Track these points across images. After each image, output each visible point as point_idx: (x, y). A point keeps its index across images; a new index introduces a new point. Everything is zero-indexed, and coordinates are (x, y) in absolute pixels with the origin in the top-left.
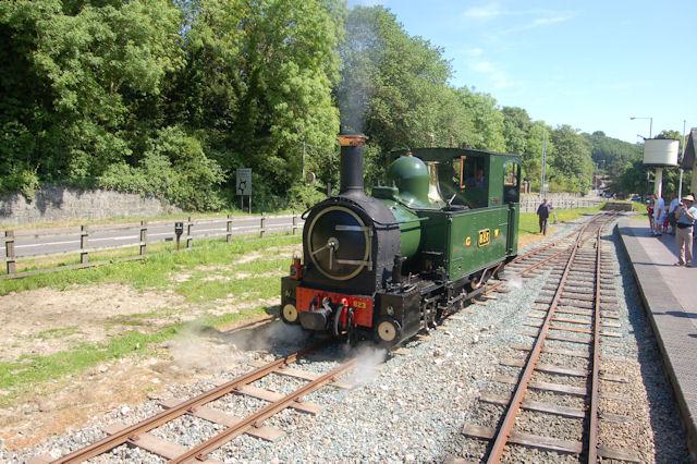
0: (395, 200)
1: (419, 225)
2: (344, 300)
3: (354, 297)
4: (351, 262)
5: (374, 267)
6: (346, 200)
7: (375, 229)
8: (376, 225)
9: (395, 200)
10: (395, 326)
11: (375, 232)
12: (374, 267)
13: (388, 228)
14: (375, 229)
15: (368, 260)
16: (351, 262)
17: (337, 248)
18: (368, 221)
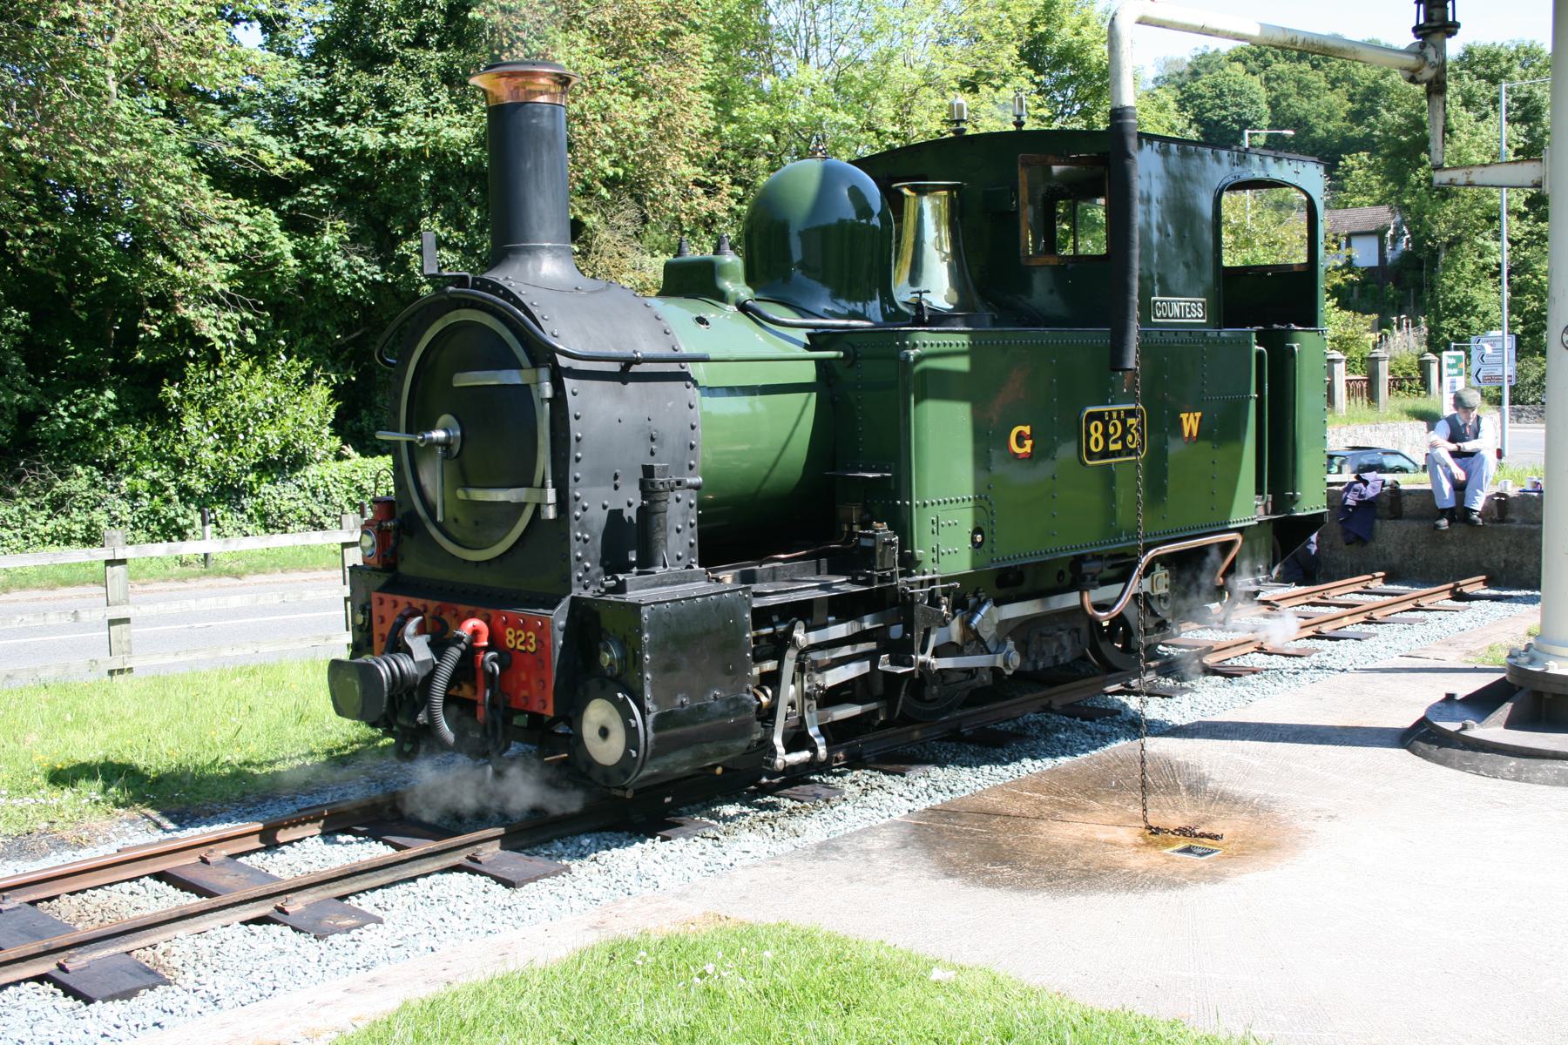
0: (721, 297)
1: (808, 373)
2: (472, 623)
3: (505, 614)
4: (500, 496)
5: (563, 504)
6: (496, 288)
7: (557, 376)
8: (563, 361)
9: (721, 297)
10: (626, 715)
11: (558, 387)
12: (563, 504)
13: (626, 371)
14: (557, 376)
15: (543, 486)
16: (500, 496)
17: (456, 449)
18: (542, 354)
